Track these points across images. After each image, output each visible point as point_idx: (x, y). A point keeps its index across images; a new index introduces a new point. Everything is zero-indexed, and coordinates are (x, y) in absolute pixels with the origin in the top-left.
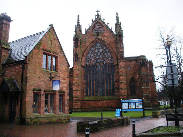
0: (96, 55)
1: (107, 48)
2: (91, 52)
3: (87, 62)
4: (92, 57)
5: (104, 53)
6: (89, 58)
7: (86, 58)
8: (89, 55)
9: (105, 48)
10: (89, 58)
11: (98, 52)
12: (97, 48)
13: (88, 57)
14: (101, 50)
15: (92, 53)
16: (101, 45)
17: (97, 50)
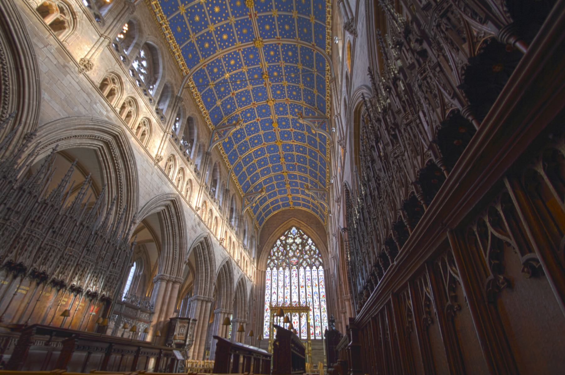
0: (289, 250)
1: (309, 237)
2: (279, 242)
3: (270, 263)
4: (280, 253)
5: (303, 245)
6: (274, 255)
7: (270, 254)
8: (275, 249)
9: (305, 237)
10: (275, 256)
11: (291, 245)
12: (289, 237)
13: (274, 253)
14: (298, 241)
15: (280, 245)
16: (298, 231)
17: (290, 241)
